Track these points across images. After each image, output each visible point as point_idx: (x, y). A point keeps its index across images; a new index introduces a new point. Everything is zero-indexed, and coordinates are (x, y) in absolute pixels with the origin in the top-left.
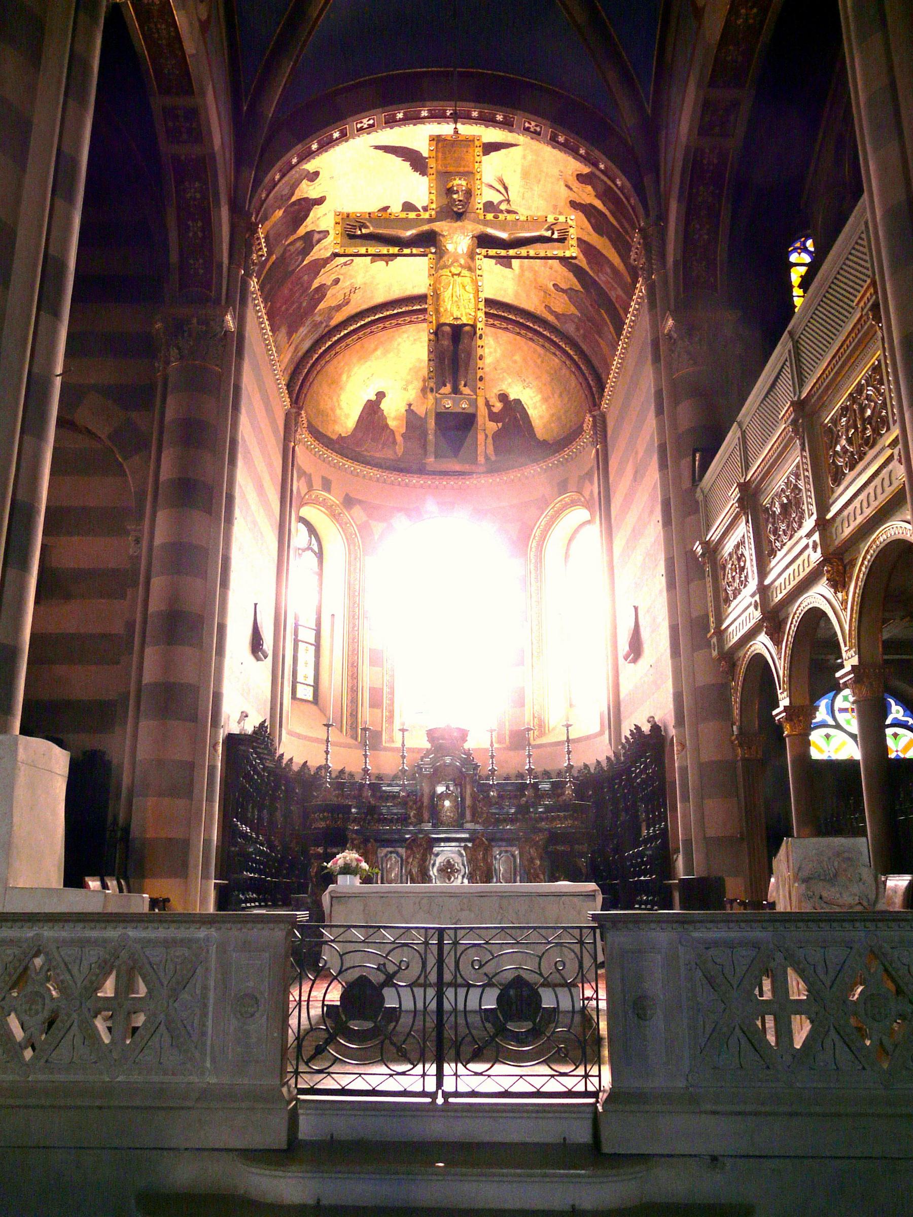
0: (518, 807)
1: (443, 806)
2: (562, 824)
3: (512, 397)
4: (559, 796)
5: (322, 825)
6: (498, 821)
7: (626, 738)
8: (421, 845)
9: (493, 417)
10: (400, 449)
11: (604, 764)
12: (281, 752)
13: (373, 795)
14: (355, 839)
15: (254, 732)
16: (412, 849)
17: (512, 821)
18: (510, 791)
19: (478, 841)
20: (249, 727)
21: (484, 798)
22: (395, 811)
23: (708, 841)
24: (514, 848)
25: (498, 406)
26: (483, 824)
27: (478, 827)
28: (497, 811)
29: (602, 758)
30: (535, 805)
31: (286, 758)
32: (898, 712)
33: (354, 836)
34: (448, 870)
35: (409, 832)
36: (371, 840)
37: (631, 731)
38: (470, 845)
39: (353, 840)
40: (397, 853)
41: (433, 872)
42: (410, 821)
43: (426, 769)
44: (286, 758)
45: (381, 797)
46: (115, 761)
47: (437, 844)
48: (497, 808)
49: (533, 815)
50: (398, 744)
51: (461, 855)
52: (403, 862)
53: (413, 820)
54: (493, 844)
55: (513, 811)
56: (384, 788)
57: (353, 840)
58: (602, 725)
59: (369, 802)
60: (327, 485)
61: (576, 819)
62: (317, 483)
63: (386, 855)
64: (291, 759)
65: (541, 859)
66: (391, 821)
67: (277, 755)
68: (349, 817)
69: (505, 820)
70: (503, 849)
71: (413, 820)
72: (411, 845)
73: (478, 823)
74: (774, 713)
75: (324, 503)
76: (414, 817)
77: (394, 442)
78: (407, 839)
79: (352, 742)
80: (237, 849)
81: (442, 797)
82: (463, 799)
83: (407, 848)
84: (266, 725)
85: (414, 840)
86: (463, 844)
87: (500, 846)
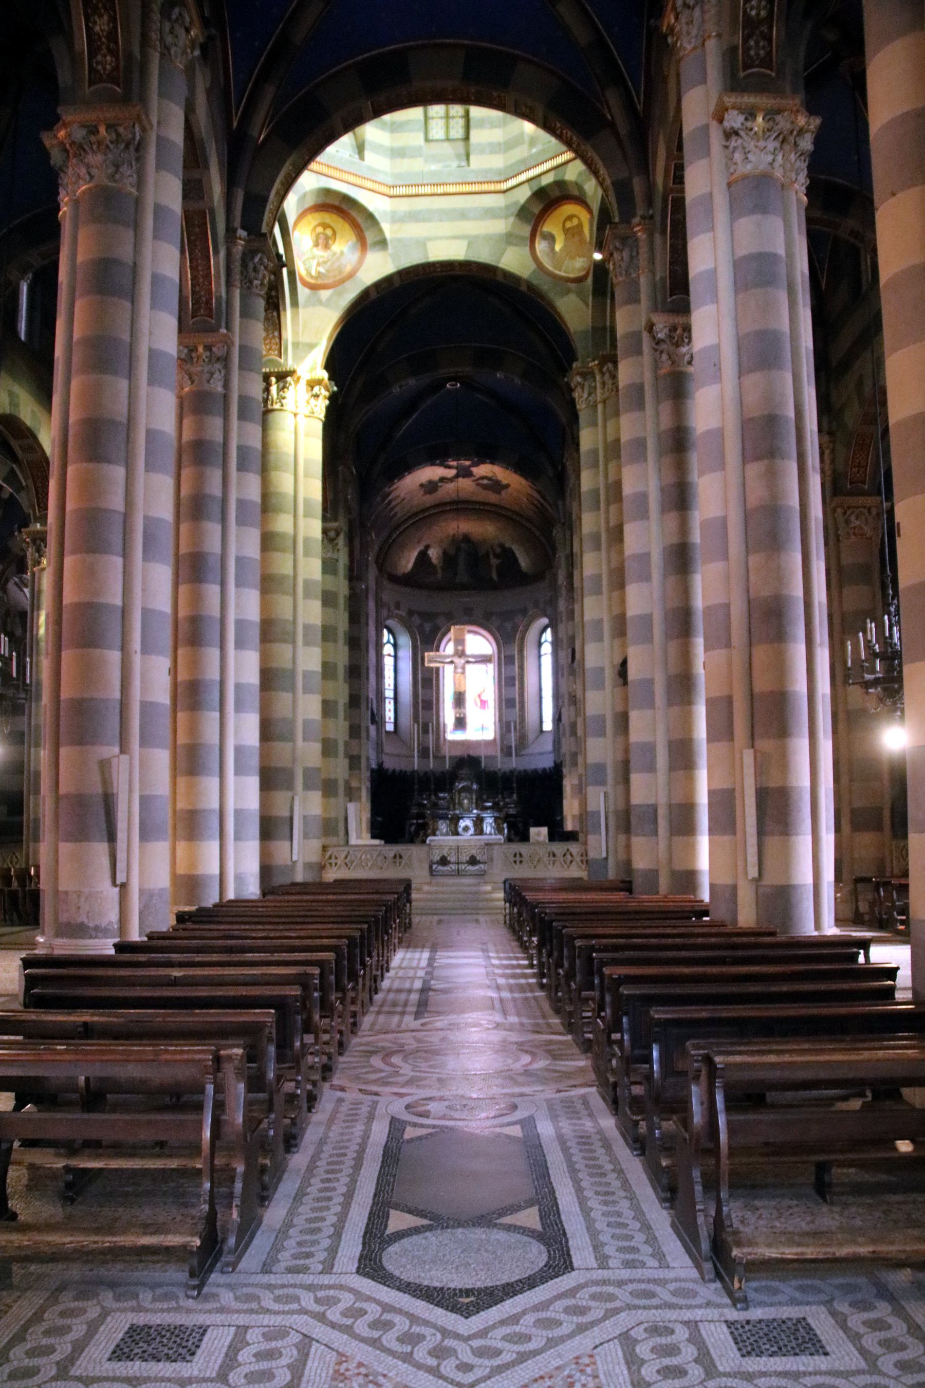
3: (507, 545)
9: (497, 556)
10: (439, 575)
25: (498, 550)
34: (466, 829)
41: (460, 830)
52: (449, 826)
60: (398, 606)
62: (392, 608)
72: (451, 820)
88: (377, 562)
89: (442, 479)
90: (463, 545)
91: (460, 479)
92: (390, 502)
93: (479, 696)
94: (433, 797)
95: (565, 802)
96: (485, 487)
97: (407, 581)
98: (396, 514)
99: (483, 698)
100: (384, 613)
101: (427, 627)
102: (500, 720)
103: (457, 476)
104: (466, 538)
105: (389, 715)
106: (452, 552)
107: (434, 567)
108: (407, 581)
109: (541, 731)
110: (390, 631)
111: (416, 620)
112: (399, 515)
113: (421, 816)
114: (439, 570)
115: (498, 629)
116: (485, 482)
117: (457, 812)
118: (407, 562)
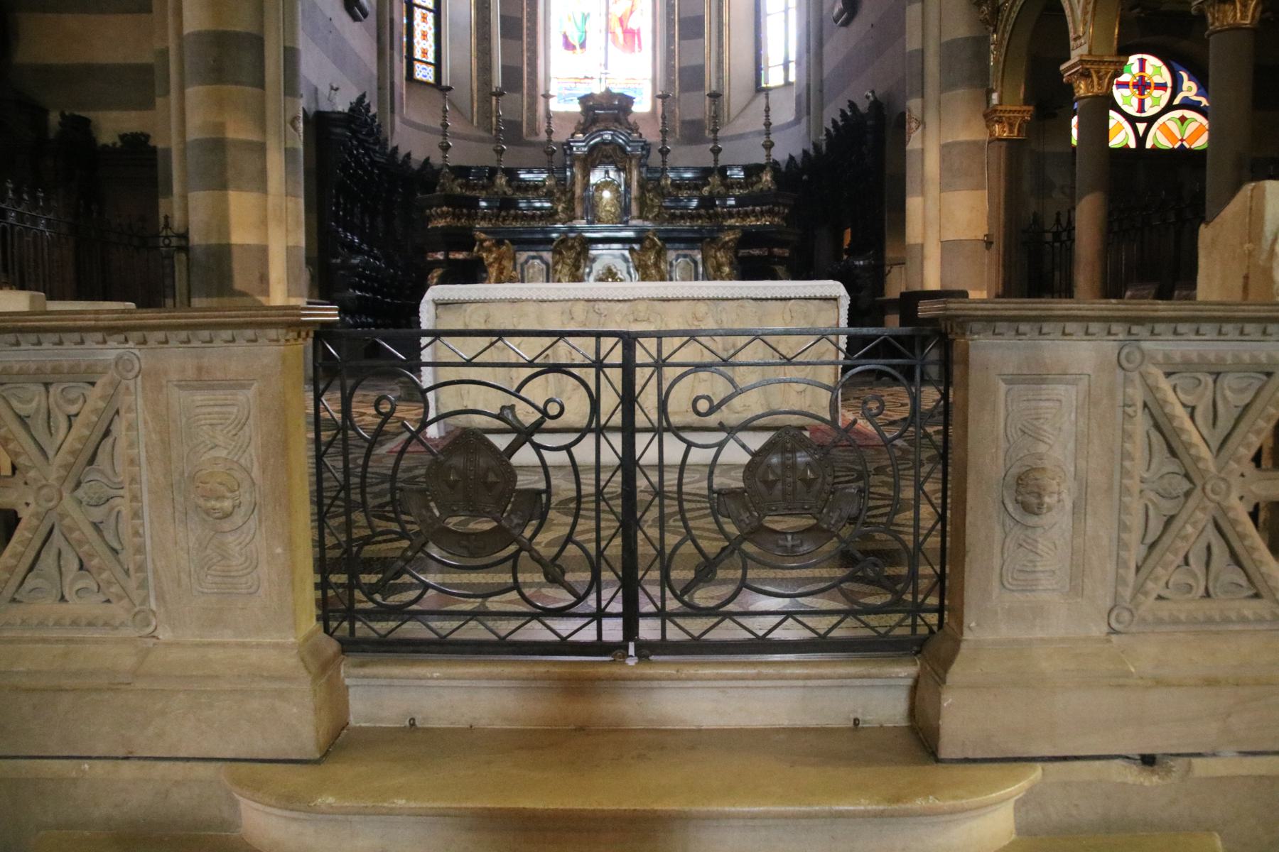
0: (702, 200)
1: (601, 198)
2: (757, 221)
4: (752, 184)
5: (441, 223)
6: (673, 217)
7: (834, 122)
8: (572, 247)
11: (799, 160)
12: (395, 145)
13: (509, 183)
14: (485, 240)
15: (351, 109)
16: (560, 253)
17: (692, 217)
18: (688, 179)
19: (647, 243)
20: (342, 105)
21: (654, 188)
22: (538, 205)
23: (948, 247)
24: (696, 252)
26: (655, 218)
27: (648, 224)
28: (672, 205)
29: (797, 153)
30: (724, 198)
31: (402, 152)
32: (1190, 89)
33: (483, 236)
35: (556, 230)
36: (507, 241)
37: (843, 111)
38: (636, 247)
39: (482, 241)
40: (541, 258)
42: (557, 217)
43: (578, 148)
44: (402, 152)
45: (519, 188)
46: (160, 146)
47: (594, 246)
48: (671, 201)
49: (719, 209)
50: (543, 136)
51: (626, 260)
53: (562, 215)
54: (668, 246)
55: (694, 203)
56: (522, 176)
57: (482, 241)
58: (798, 111)
59: (505, 193)
61: (776, 214)
63: (526, 262)
64: (408, 155)
65: (731, 264)
66: (533, 217)
67: (390, 148)
68: (477, 213)
69: (682, 217)
70: (680, 252)
71: (562, 215)
72: (560, 247)
73: (646, 219)
74: (1063, 67)
76: (563, 212)
78: (552, 240)
79: (486, 135)
80: (339, 261)
81: (599, 187)
82: (628, 185)
83: (555, 251)
84: (367, 101)
85: (563, 241)
86: (627, 246)
87: (677, 249)
93: (621, 20)
94: (501, 180)
95: (914, 204)
99: (632, 24)
102: (669, 68)
105: (424, 45)
109: (759, 89)
113: (463, 239)
117: (581, 224)
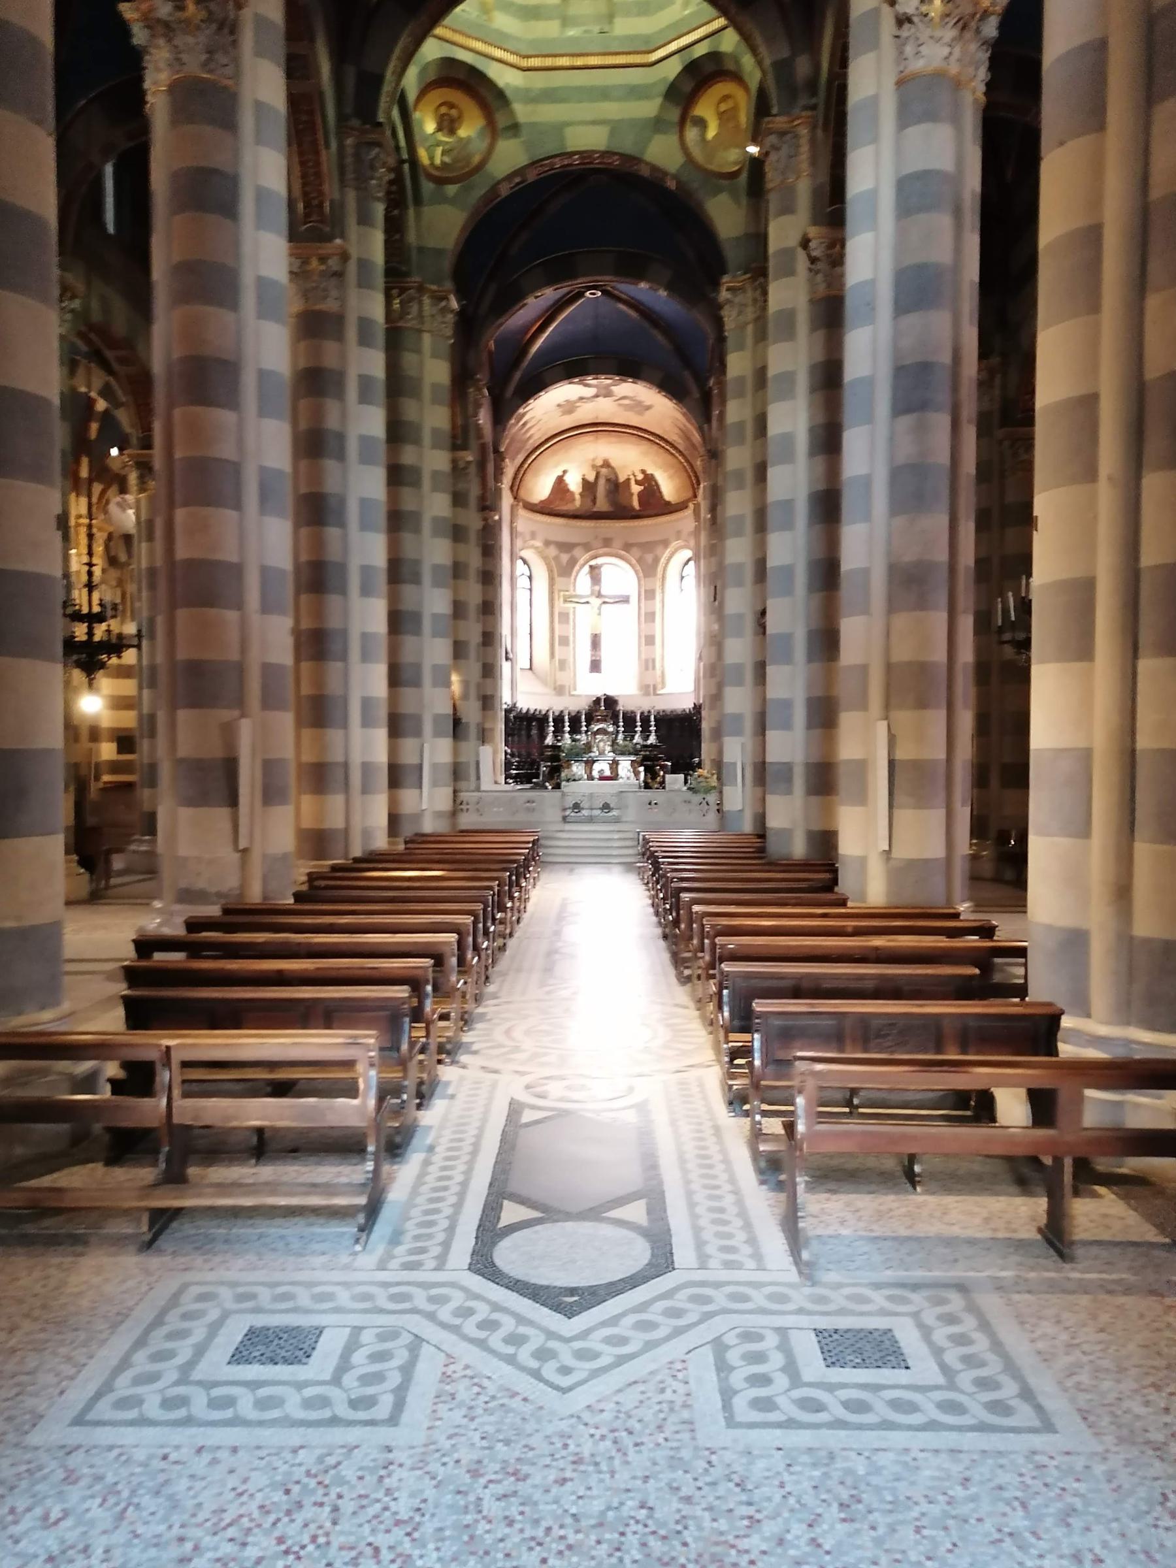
3: (649, 472)
9: (638, 483)
10: (578, 503)
60: (533, 535)
72: (586, 762)
75: (532, 547)
77: (574, 500)
88: (511, 488)
89: (581, 398)
90: (604, 471)
91: (600, 399)
92: (524, 424)
96: (628, 408)
97: (544, 509)
98: (530, 438)
100: (519, 543)
101: (565, 557)
103: (597, 396)
104: (606, 464)
106: (591, 477)
107: (572, 494)
108: (544, 509)
110: (525, 562)
111: (552, 551)
112: (536, 437)
114: (577, 497)
115: (639, 561)
116: (626, 402)
118: (541, 488)
